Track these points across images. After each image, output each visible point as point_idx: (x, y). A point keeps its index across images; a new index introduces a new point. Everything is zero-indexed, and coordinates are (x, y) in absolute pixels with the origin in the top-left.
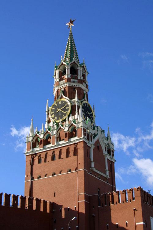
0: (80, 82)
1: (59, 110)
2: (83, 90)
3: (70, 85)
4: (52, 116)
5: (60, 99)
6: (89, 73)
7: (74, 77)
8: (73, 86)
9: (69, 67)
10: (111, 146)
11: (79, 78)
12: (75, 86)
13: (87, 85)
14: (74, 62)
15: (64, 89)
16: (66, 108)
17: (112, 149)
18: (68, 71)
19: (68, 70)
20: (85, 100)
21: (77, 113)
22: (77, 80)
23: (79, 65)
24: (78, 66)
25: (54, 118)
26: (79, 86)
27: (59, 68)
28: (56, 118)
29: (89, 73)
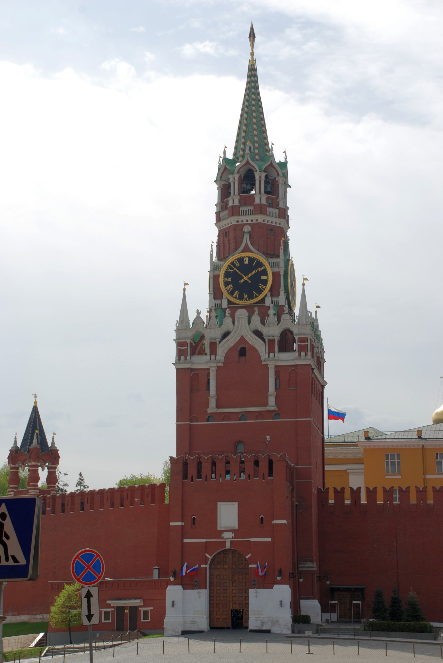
1: (246, 278)
3: (264, 221)
4: (228, 287)
5: (243, 251)
6: (290, 187)
7: (270, 201)
8: (270, 223)
11: (281, 205)
12: (274, 224)
15: (252, 228)
16: (262, 278)
19: (260, 182)
21: (282, 293)
22: (276, 211)
23: (281, 174)
24: (278, 175)
25: (232, 293)
27: (238, 172)
28: (236, 293)
29: (290, 187)
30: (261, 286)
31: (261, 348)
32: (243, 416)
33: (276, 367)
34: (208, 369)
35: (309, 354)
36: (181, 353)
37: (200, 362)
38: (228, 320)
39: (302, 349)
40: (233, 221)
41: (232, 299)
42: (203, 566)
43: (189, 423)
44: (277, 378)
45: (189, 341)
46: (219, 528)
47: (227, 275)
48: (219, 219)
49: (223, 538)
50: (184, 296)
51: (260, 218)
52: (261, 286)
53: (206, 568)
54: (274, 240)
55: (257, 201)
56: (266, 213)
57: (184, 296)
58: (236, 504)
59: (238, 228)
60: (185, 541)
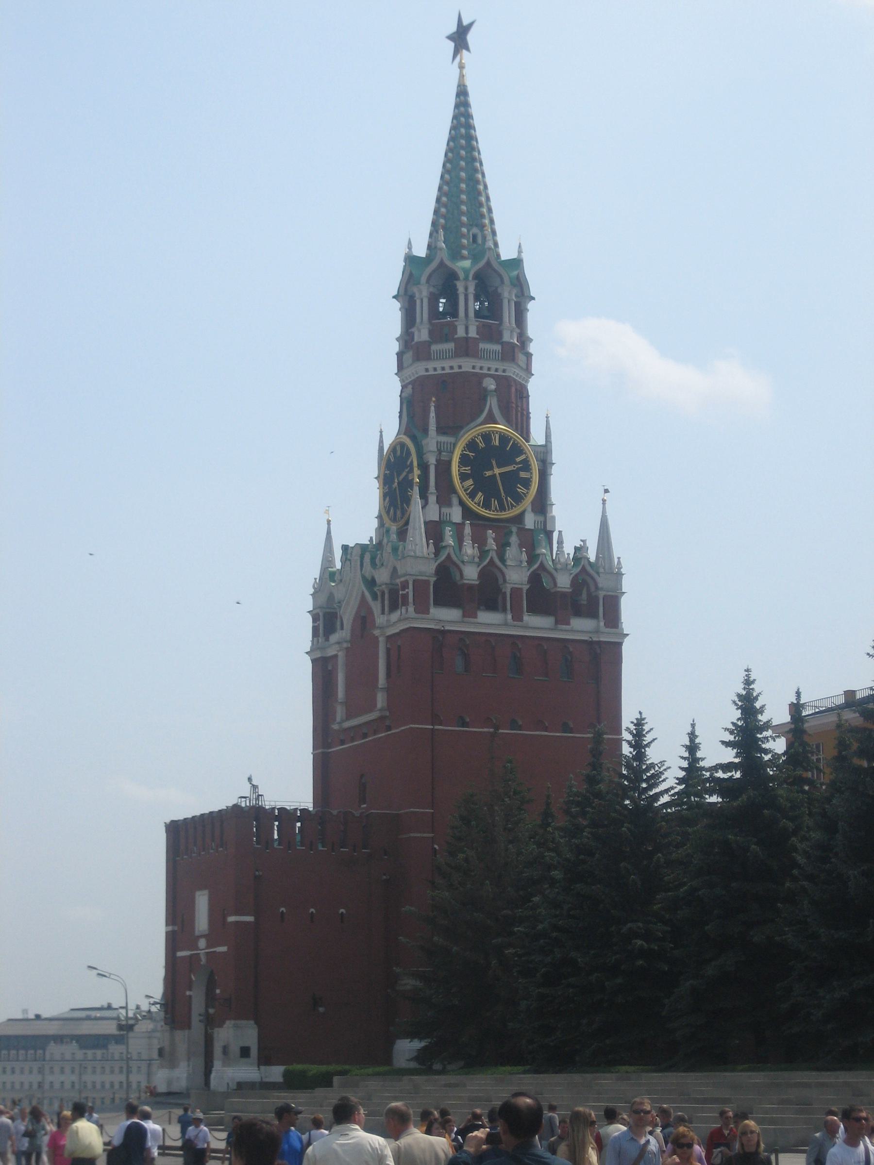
0: (466, 348)
2: (480, 377)
3: (427, 370)
8: (439, 372)
9: (425, 293)
10: (602, 581)
11: (461, 332)
12: (448, 371)
13: (503, 344)
14: (442, 264)
17: (601, 594)
18: (423, 312)
20: (491, 419)
22: (450, 346)
25: (388, 512)
26: (460, 367)
31: (376, 607)
33: (389, 638)
34: (336, 656)
35: (411, 609)
42: (188, 993)
43: (320, 751)
45: (318, 611)
46: (197, 933)
49: (197, 949)
50: (329, 532)
51: (420, 369)
53: (190, 996)
56: (428, 358)
57: (329, 532)
58: (206, 892)
60: (180, 954)
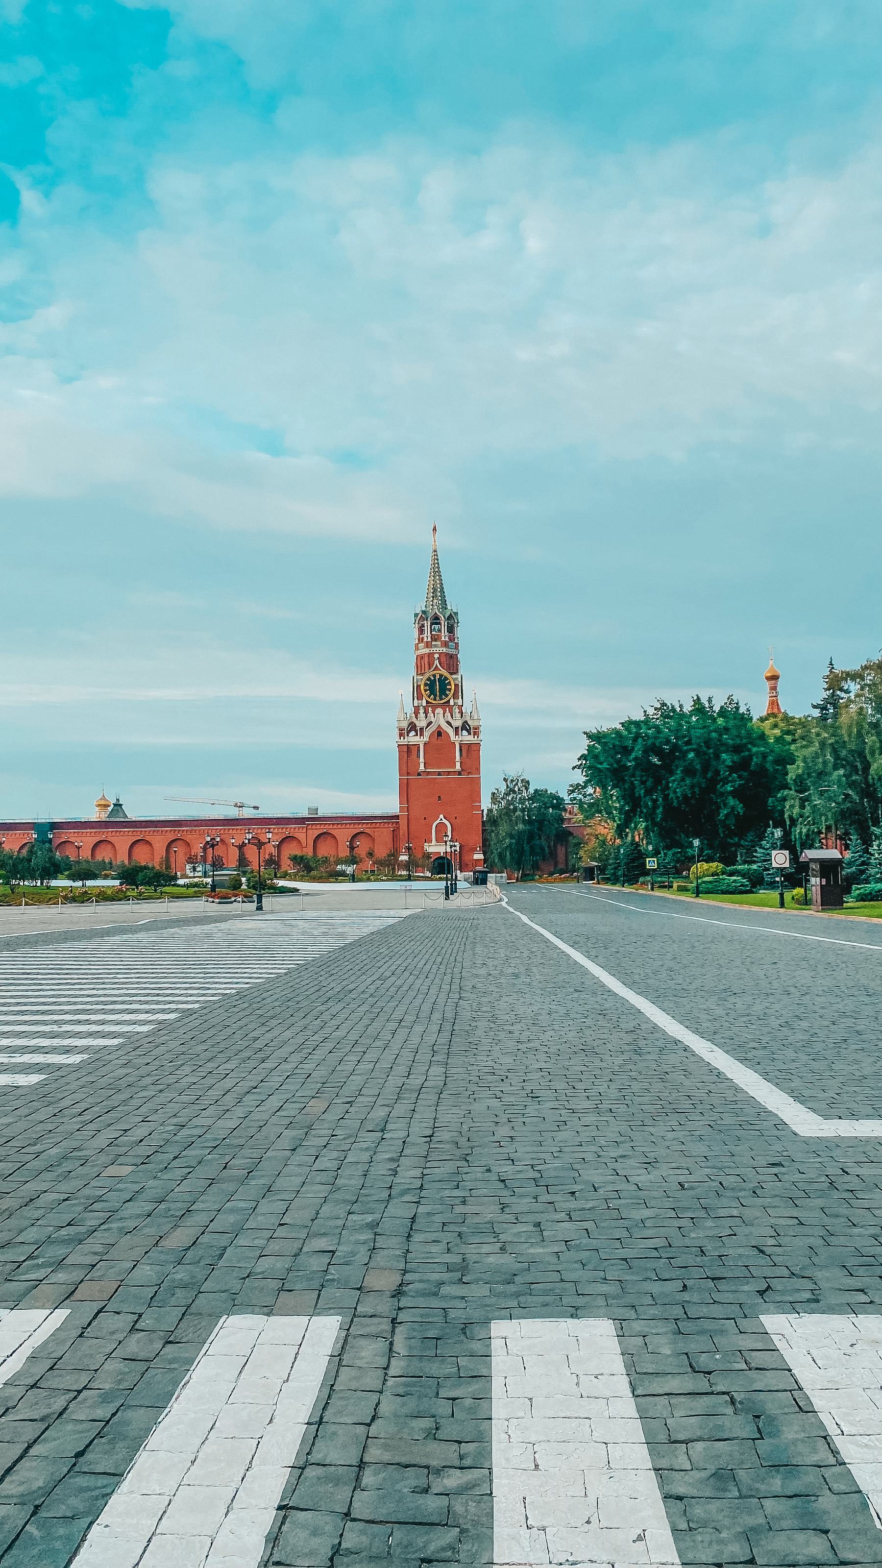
25: (429, 697)
30: (448, 692)
32: (439, 774)
36: (401, 735)
37: (413, 739)
38: (431, 714)
39: (475, 733)
40: (427, 651)
41: (429, 700)
44: (461, 750)
47: (426, 685)
48: (417, 649)
52: (448, 692)
54: (451, 662)
55: (443, 639)
59: (430, 655)
